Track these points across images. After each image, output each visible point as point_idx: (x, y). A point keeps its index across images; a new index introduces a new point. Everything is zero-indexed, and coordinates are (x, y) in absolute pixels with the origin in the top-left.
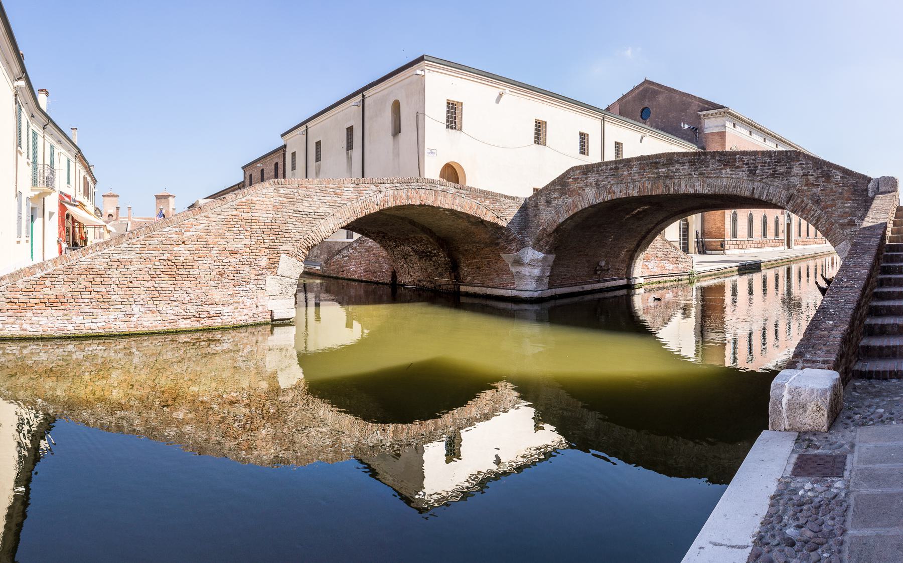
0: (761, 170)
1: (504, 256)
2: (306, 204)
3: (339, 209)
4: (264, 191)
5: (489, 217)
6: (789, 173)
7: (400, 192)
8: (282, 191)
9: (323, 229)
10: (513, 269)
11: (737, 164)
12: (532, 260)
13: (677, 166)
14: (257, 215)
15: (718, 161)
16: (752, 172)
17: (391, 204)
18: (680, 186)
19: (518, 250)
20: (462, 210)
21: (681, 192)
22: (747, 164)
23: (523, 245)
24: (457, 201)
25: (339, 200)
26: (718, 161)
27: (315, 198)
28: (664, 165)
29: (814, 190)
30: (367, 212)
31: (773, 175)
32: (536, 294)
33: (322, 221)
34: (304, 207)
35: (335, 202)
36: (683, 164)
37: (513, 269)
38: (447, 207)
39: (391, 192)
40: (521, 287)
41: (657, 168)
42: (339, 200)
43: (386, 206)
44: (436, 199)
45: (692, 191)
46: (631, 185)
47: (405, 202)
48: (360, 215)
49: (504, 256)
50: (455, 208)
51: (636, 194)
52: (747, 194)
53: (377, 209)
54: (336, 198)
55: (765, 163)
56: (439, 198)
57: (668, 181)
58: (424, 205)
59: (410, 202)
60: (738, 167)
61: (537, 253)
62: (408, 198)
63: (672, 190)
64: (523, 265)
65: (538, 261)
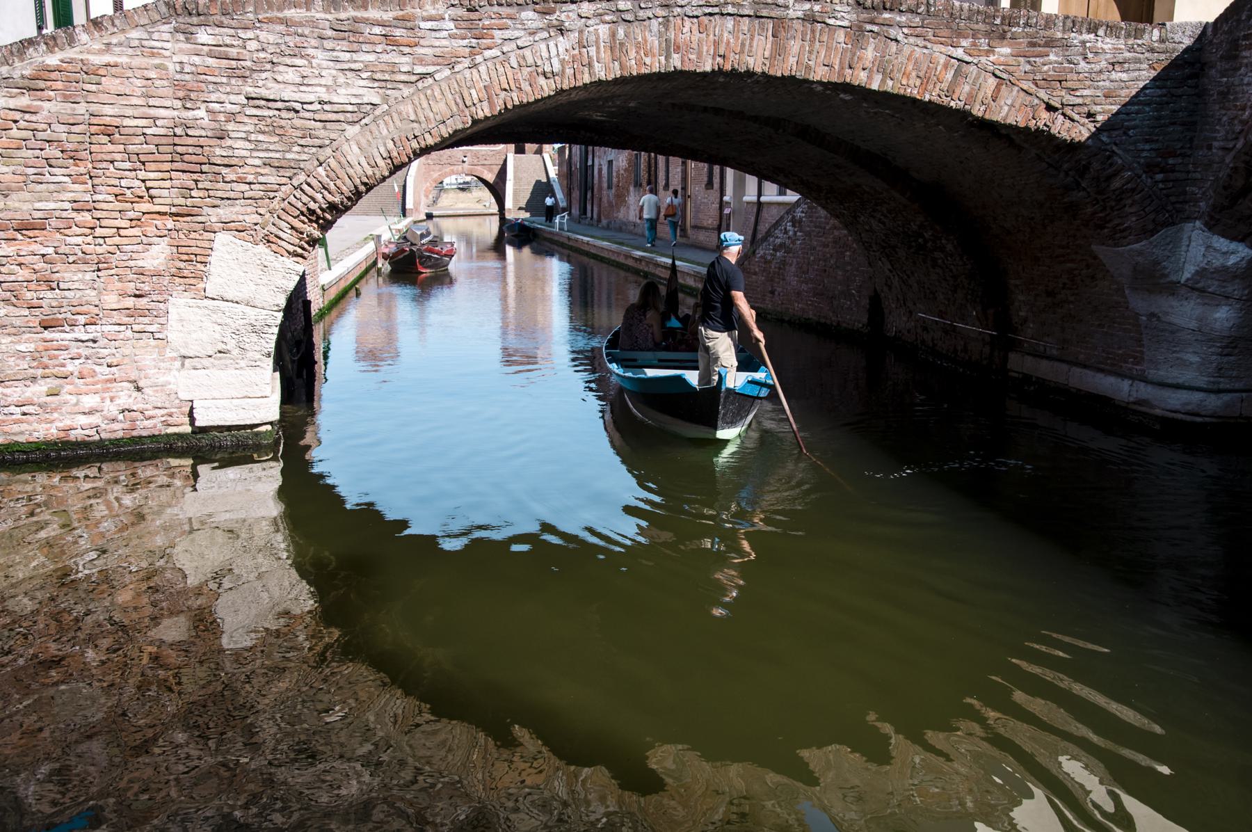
1: (1102, 251)
2: (291, 75)
3: (406, 91)
4: (135, 34)
5: (1008, 110)
7: (637, 29)
8: (203, 36)
9: (353, 153)
10: (1139, 303)
12: (1201, 273)
14: (108, 110)
17: (602, 72)
19: (1147, 233)
20: (889, 86)
23: (1167, 214)
24: (869, 54)
25: (404, 63)
27: (319, 54)
30: (516, 98)
32: (1213, 403)
33: (352, 131)
34: (283, 84)
35: (393, 68)
37: (1139, 303)
38: (820, 74)
39: (603, 30)
40: (1164, 373)
42: (404, 63)
43: (587, 79)
44: (779, 51)
47: (655, 64)
48: (484, 111)
49: (1102, 251)
50: (861, 78)
53: (547, 88)
54: (394, 57)
56: (794, 46)
58: (734, 73)
59: (676, 62)
61: (1221, 243)
62: (669, 48)
64: (1172, 289)
65: (1225, 274)
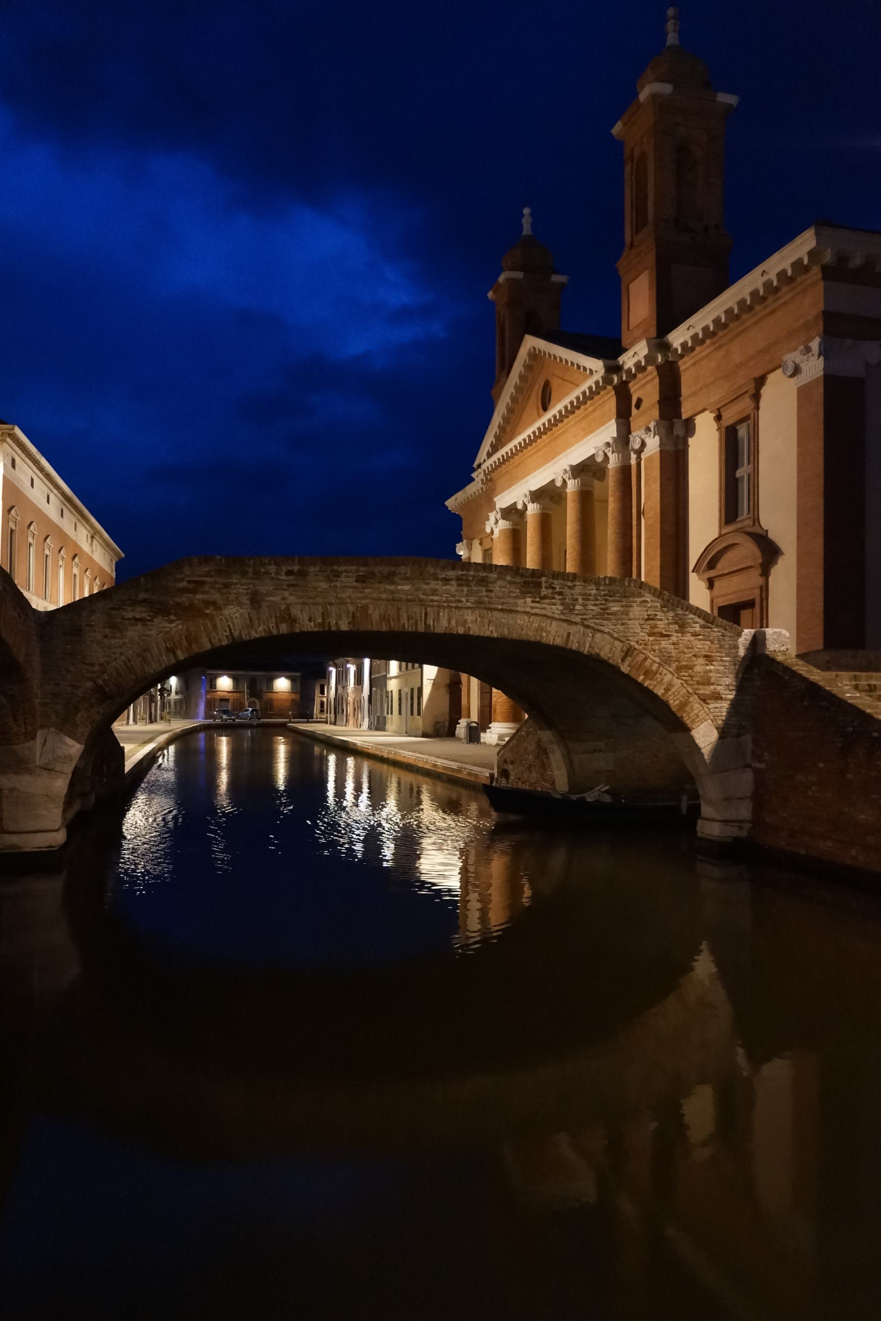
0: (584, 605)
6: (627, 614)
11: (544, 592)
13: (433, 584)
15: (510, 582)
16: (569, 608)
18: (437, 619)
21: (439, 630)
22: (560, 593)
26: (510, 582)
28: (407, 579)
29: (664, 643)
31: (605, 613)
36: (446, 581)
41: (393, 583)
45: (461, 630)
46: (333, 609)
51: (344, 627)
52: (559, 641)
55: (590, 595)
57: (416, 609)
60: (545, 597)
63: (421, 628)
